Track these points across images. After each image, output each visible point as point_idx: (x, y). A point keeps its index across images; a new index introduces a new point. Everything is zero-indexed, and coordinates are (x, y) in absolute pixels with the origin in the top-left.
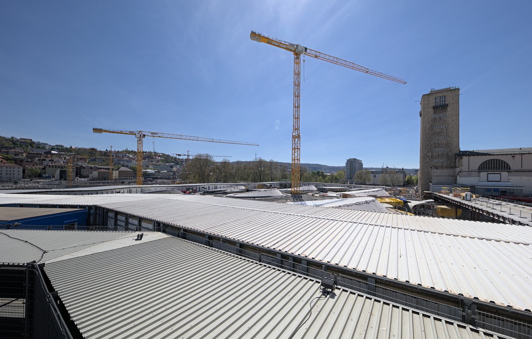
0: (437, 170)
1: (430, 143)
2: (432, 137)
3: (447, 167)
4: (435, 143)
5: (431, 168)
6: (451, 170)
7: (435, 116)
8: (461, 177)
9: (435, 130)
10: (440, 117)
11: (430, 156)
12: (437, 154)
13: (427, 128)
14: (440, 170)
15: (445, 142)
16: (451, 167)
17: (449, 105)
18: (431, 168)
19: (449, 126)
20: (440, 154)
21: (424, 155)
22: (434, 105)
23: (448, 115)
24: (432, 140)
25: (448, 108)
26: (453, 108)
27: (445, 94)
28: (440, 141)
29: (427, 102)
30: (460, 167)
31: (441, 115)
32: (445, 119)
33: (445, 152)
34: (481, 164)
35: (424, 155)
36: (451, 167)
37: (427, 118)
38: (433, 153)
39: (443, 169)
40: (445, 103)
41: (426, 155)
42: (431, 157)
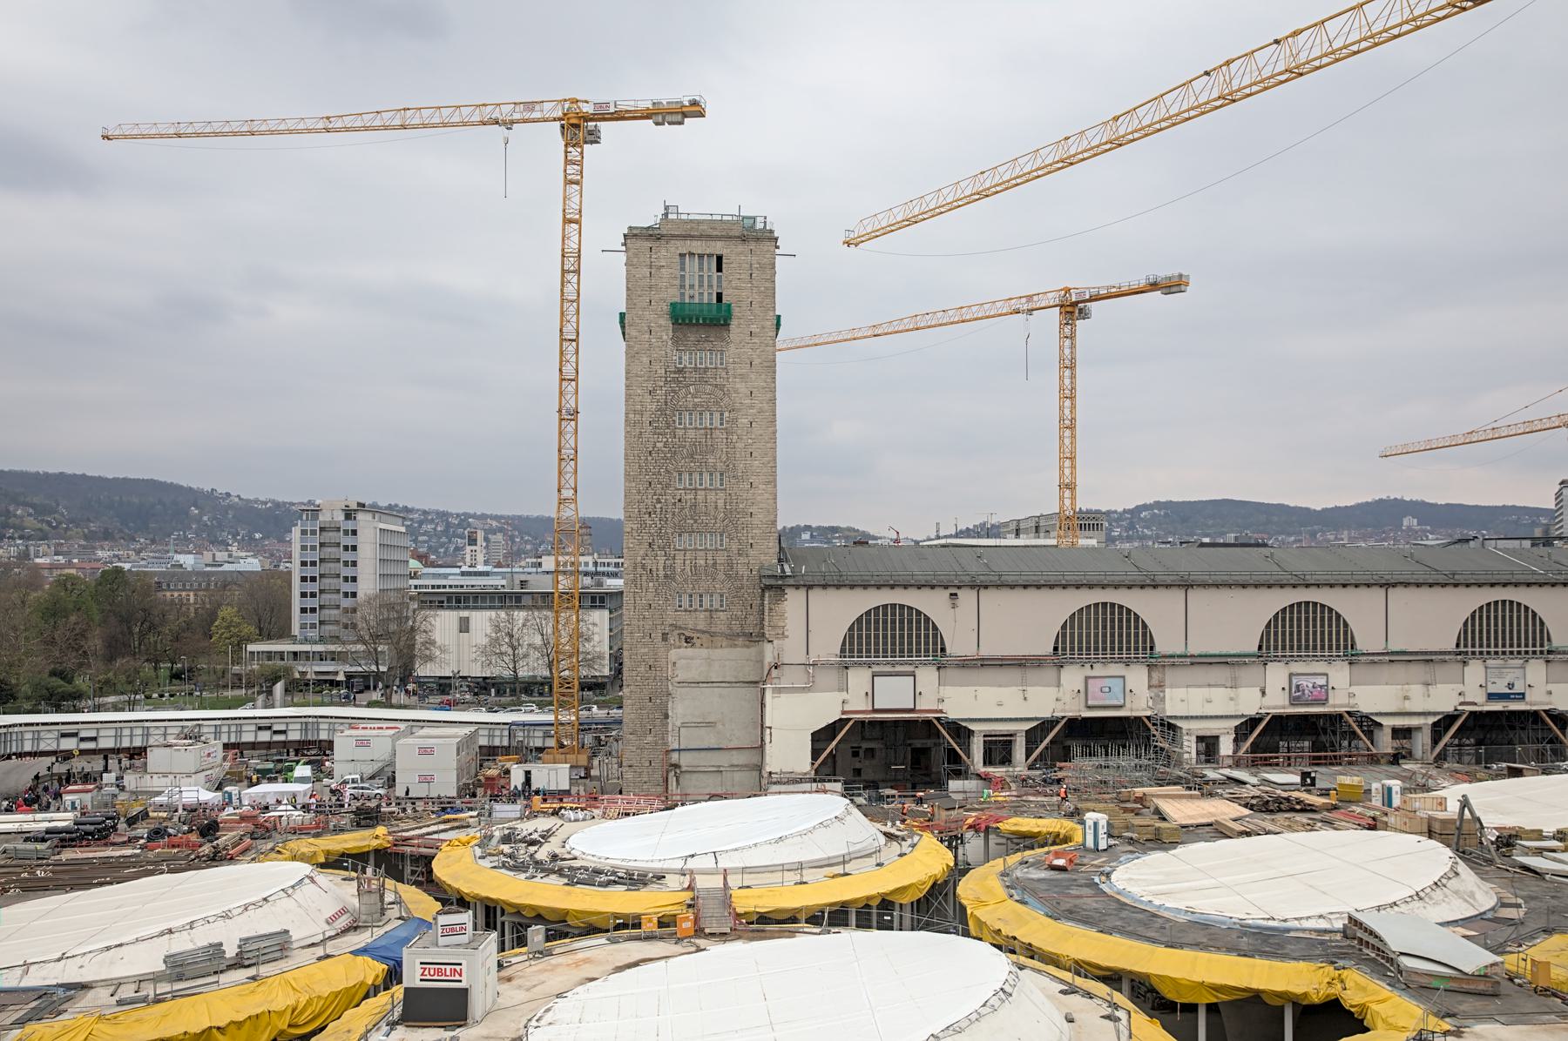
0: (690, 651)
1: (659, 501)
2: (667, 471)
3: (732, 637)
4: (680, 501)
5: (665, 637)
6: (745, 649)
7: (680, 358)
8: (779, 691)
9: (680, 433)
10: (701, 363)
11: (661, 573)
12: (688, 562)
13: (647, 419)
14: (704, 652)
15: (721, 503)
16: (744, 635)
18: (665, 637)
19: (734, 421)
20: (702, 562)
21: (635, 568)
22: (673, 295)
23: (734, 363)
24: (668, 486)
25: (734, 323)
26: (754, 328)
28: (700, 497)
29: (646, 271)
30: (775, 642)
31: (706, 359)
33: (721, 559)
34: (851, 629)
35: (635, 568)
36: (744, 635)
39: (716, 648)
42: (666, 576)
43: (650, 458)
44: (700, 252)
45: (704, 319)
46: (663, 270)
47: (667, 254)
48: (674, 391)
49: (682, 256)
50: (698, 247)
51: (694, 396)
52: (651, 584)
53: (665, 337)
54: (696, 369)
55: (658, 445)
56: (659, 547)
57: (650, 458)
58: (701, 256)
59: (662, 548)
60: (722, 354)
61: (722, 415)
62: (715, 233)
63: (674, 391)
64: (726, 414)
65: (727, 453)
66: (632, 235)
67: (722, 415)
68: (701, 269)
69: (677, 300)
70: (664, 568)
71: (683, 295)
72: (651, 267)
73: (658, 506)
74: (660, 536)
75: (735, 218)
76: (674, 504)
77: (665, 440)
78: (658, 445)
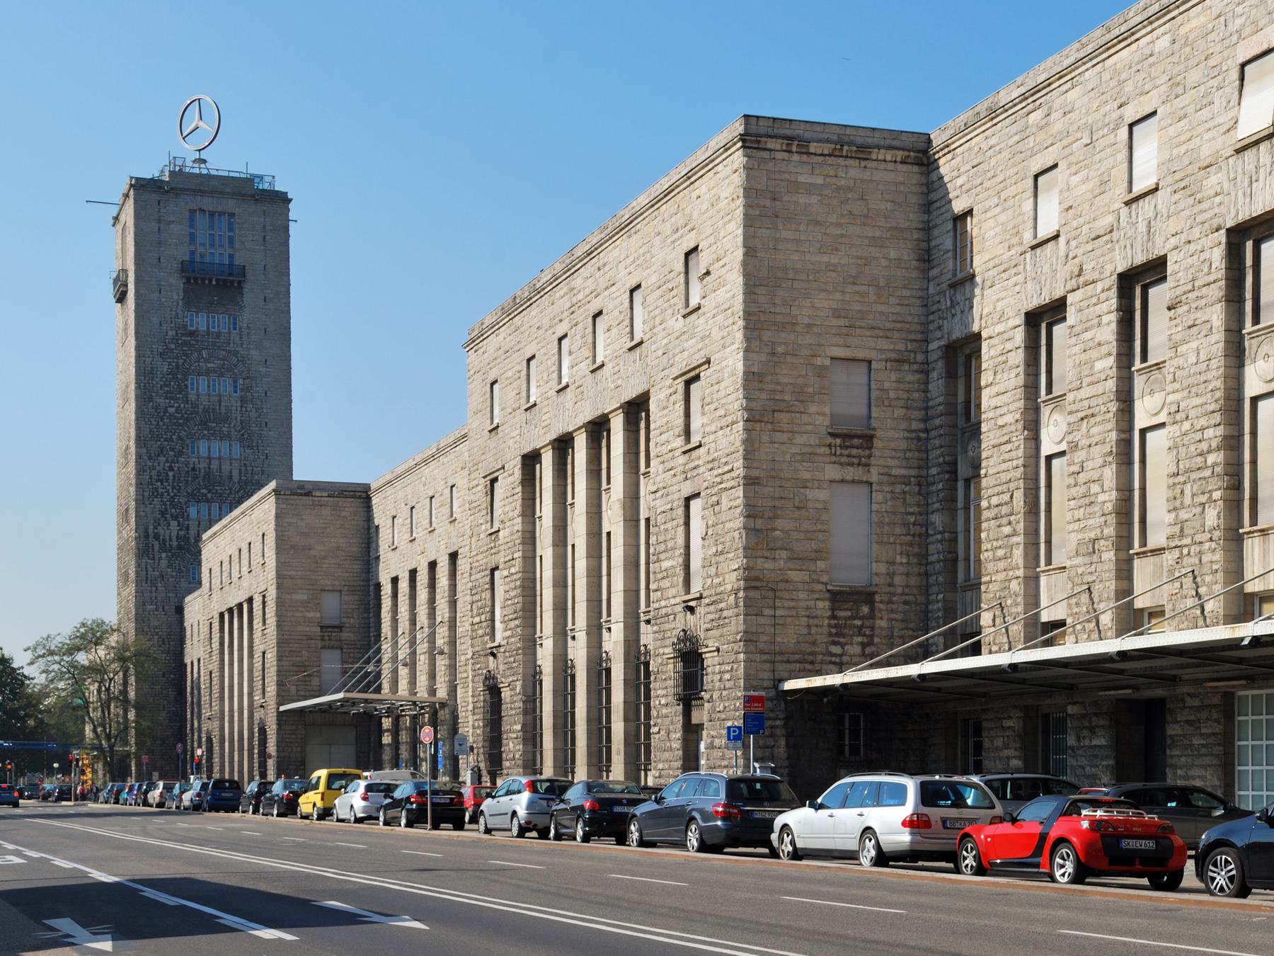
1: (171, 469)
2: (180, 438)
4: (193, 469)
9: (192, 398)
10: (214, 327)
11: (175, 544)
15: (235, 473)
17: (249, 275)
24: (180, 453)
25: (247, 287)
27: (230, 205)
32: (231, 347)
37: (155, 320)
38: (188, 528)
40: (231, 256)
41: (156, 536)
42: (179, 547)
43: (161, 424)
44: (211, 209)
45: (218, 281)
46: (173, 226)
47: (177, 209)
48: (186, 355)
49: (192, 212)
50: (208, 203)
51: (207, 361)
52: (164, 555)
53: (176, 297)
54: (208, 333)
55: (171, 410)
56: (172, 516)
57: (161, 424)
58: (212, 214)
59: (175, 518)
60: (235, 319)
61: (235, 382)
62: (227, 190)
63: (186, 355)
64: (241, 381)
65: (242, 422)
66: (142, 187)
67: (235, 382)
68: (212, 227)
69: (187, 258)
70: (178, 538)
71: (192, 253)
72: (159, 221)
73: (171, 474)
74: (173, 505)
75: (242, 176)
76: (187, 473)
77: (176, 405)
78: (171, 410)
